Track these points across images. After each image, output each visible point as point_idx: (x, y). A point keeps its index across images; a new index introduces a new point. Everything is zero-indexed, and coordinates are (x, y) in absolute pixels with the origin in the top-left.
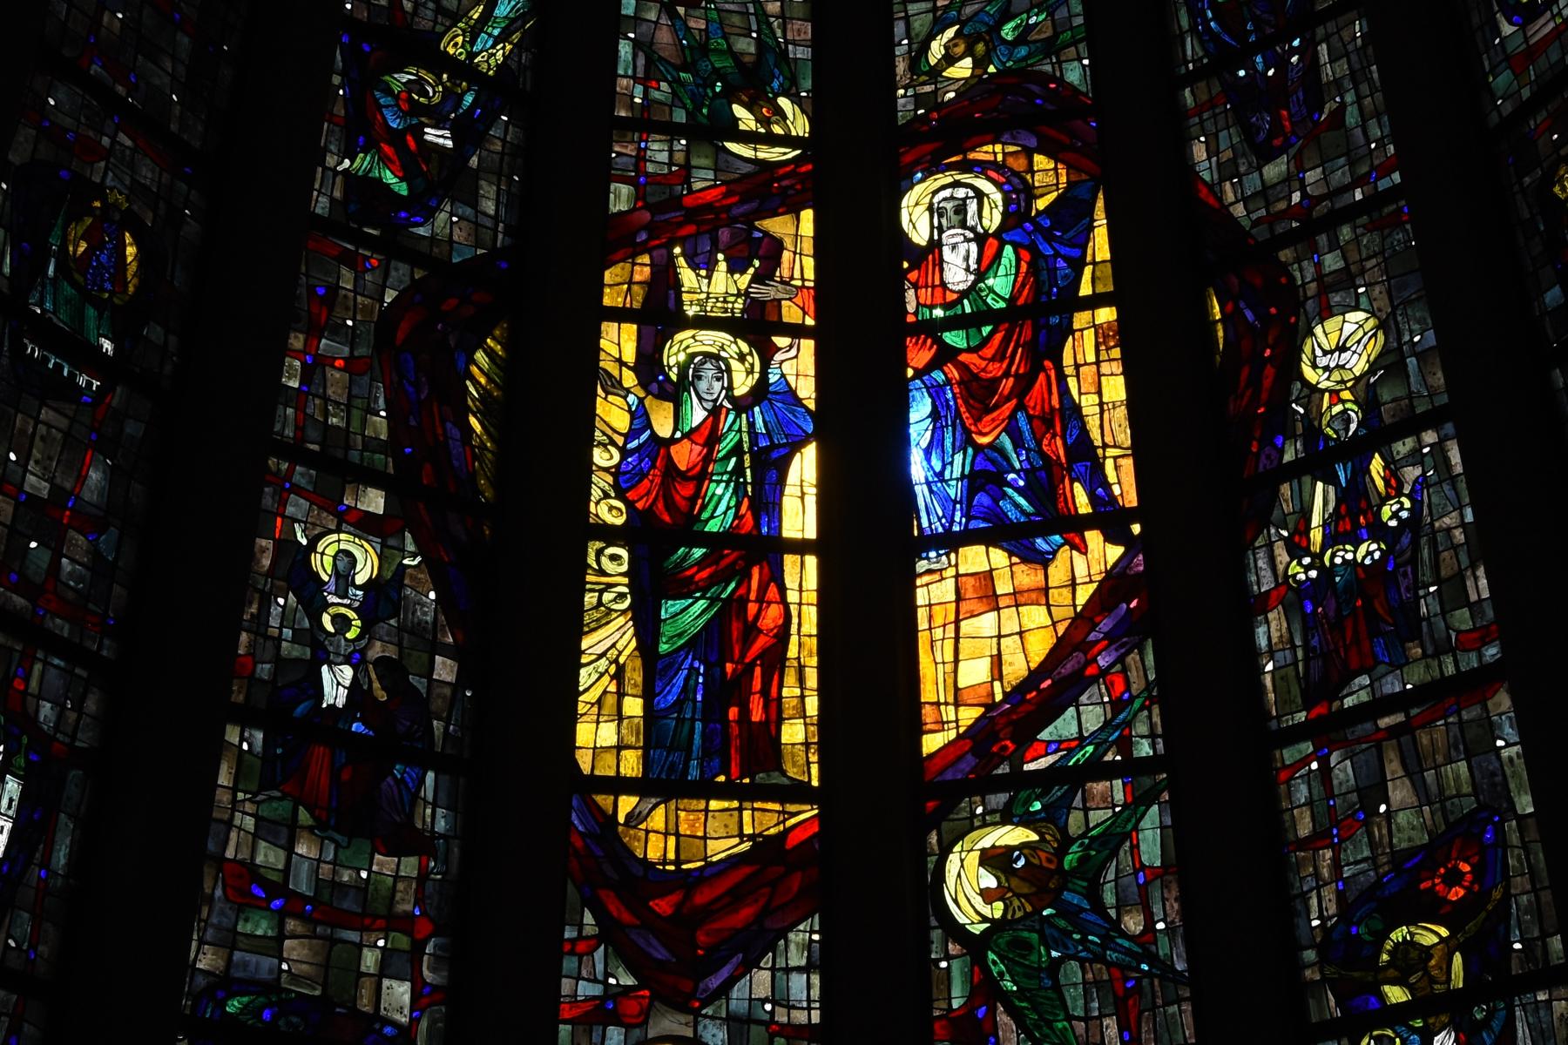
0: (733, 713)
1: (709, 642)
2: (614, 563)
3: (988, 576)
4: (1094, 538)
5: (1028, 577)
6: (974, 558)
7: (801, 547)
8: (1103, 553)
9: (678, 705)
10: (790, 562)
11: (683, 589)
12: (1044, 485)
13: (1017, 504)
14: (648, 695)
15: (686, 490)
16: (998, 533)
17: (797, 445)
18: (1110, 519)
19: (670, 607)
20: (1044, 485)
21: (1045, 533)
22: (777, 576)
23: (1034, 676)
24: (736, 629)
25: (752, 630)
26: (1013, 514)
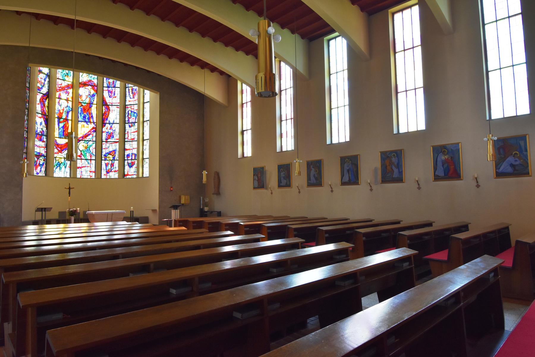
0: (65, 133)
1: (63, 127)
2: (56, 120)
3: (84, 125)
4: (92, 123)
5: (87, 125)
6: (83, 123)
7: (70, 120)
8: (92, 126)
9: (61, 132)
10: (69, 121)
11: (61, 122)
12: (89, 119)
13: (87, 120)
14: (59, 131)
15: (61, 114)
16: (85, 121)
17: (70, 111)
18: (94, 123)
19: (60, 124)
20: (89, 119)
21: (88, 122)
22: (68, 122)
23: (87, 133)
24: (65, 126)
25: (66, 126)
26: (86, 121)
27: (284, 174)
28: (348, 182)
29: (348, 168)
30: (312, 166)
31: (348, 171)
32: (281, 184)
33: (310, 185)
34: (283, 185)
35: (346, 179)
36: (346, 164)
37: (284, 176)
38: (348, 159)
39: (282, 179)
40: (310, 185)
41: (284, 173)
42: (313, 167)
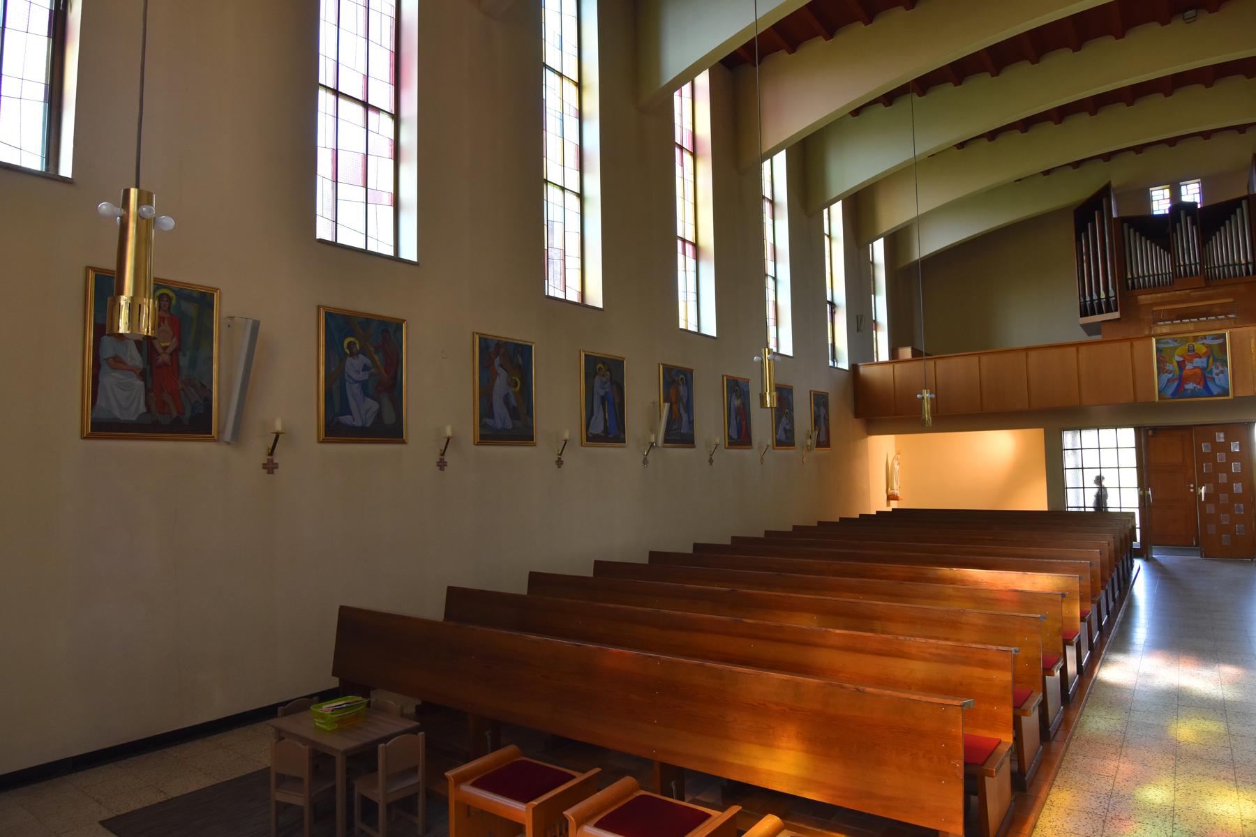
27: (365, 368)
28: (603, 434)
29: (602, 392)
30: (497, 361)
31: (603, 399)
32: (346, 419)
33: (489, 435)
34: (358, 423)
35: (598, 428)
36: (597, 378)
37: (364, 376)
38: (604, 363)
39: (353, 391)
40: (489, 435)
41: (368, 361)
42: (500, 365)
